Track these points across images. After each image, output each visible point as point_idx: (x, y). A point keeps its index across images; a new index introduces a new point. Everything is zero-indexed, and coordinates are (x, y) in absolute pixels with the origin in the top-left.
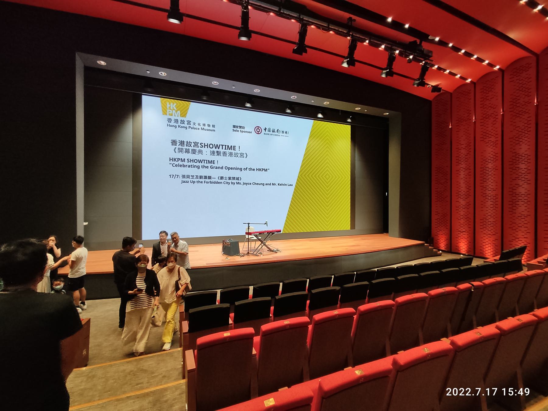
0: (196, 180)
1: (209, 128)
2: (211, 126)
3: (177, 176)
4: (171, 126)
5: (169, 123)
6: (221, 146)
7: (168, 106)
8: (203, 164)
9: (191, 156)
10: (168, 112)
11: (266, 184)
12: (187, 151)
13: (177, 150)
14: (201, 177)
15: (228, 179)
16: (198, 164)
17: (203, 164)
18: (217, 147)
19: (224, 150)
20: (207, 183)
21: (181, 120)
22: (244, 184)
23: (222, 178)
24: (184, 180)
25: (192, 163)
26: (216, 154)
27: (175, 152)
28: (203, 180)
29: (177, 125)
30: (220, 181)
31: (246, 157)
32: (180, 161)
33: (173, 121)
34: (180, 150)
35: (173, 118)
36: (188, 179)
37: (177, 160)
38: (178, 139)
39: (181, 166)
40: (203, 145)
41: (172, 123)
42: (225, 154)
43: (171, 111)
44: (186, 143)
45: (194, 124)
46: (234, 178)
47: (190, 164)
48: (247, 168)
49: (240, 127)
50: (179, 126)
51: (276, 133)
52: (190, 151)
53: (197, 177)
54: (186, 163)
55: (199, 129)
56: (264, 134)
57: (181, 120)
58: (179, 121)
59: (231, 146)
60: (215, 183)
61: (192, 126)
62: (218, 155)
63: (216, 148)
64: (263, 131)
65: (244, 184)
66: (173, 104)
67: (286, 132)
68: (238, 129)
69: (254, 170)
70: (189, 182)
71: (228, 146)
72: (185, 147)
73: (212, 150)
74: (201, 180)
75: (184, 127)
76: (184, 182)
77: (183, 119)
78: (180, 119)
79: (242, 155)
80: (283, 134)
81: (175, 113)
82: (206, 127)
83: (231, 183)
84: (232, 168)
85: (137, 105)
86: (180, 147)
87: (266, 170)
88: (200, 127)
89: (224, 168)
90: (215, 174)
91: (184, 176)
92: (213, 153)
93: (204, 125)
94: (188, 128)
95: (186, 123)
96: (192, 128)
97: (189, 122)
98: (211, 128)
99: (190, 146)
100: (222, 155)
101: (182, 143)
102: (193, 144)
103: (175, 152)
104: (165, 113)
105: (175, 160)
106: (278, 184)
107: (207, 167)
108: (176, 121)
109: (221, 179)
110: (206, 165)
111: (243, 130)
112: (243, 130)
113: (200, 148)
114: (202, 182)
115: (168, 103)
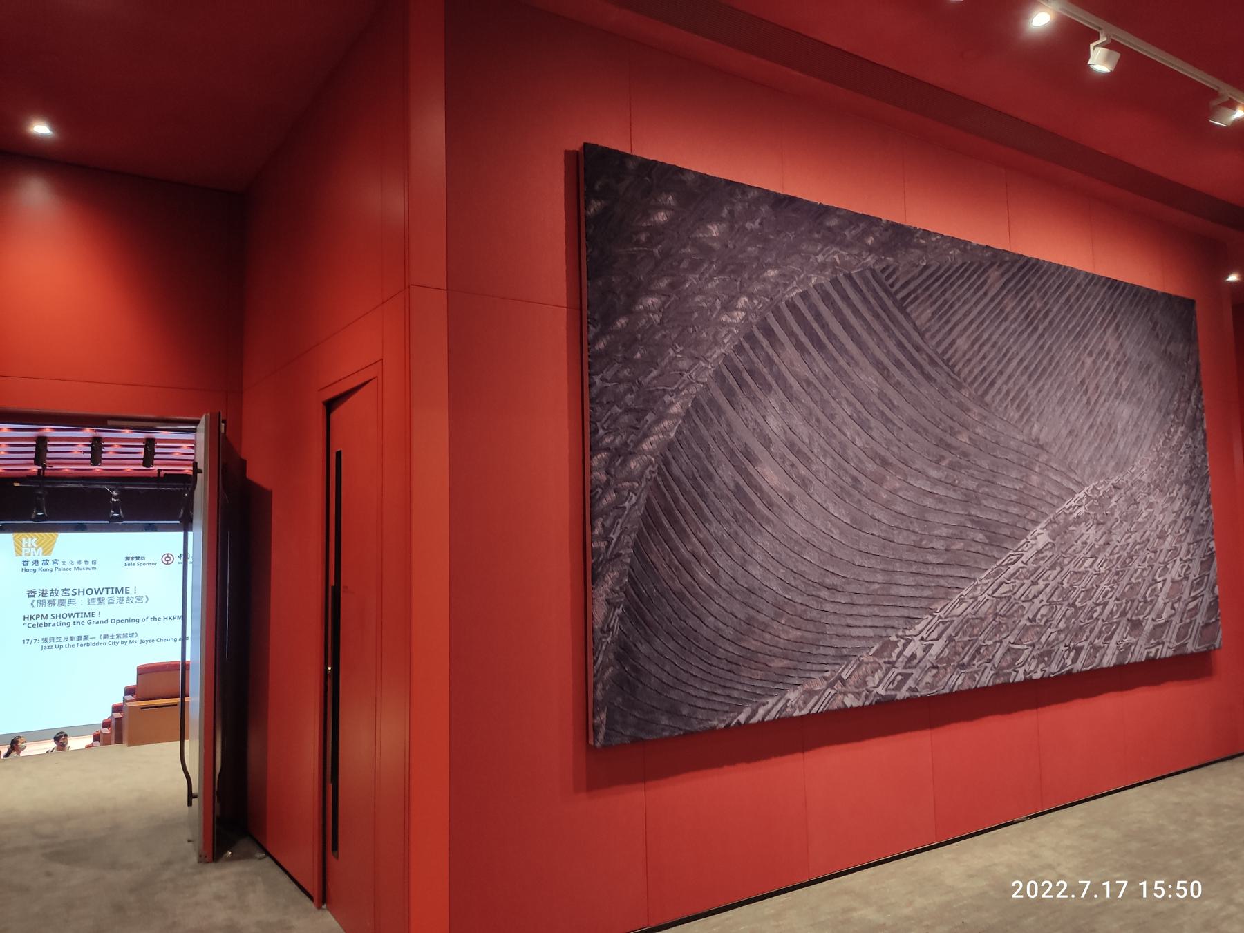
1: (86, 566)
2: (91, 562)
6: (105, 590)
20: (82, 645)
30: (103, 641)
42: (111, 600)
49: (138, 558)
63: (97, 594)
68: (133, 562)
82: (83, 565)
89: (109, 621)
98: (90, 565)
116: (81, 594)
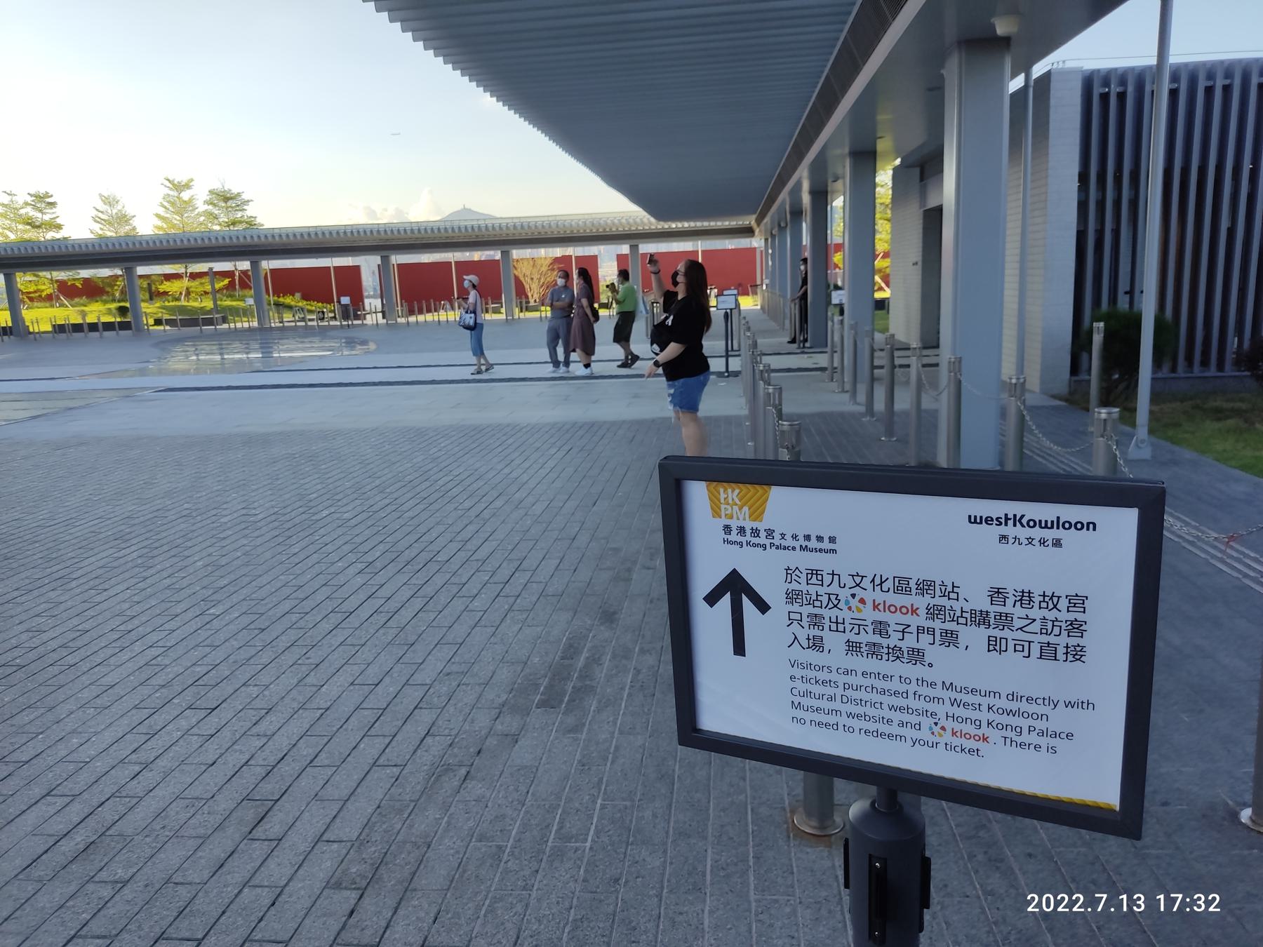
2: (826, 540)
4: (729, 542)
5: (726, 537)
7: (723, 496)
10: (723, 510)
29: (743, 540)
33: (734, 532)
35: (734, 524)
41: (734, 536)
50: (748, 543)
55: (794, 549)
57: (752, 529)
58: (748, 532)
77: (755, 525)
78: (748, 525)
81: (739, 513)
82: (813, 544)
88: (797, 545)
93: (808, 538)
94: (768, 546)
95: (763, 534)
96: (777, 548)
97: (770, 533)
98: (826, 545)
108: (742, 530)
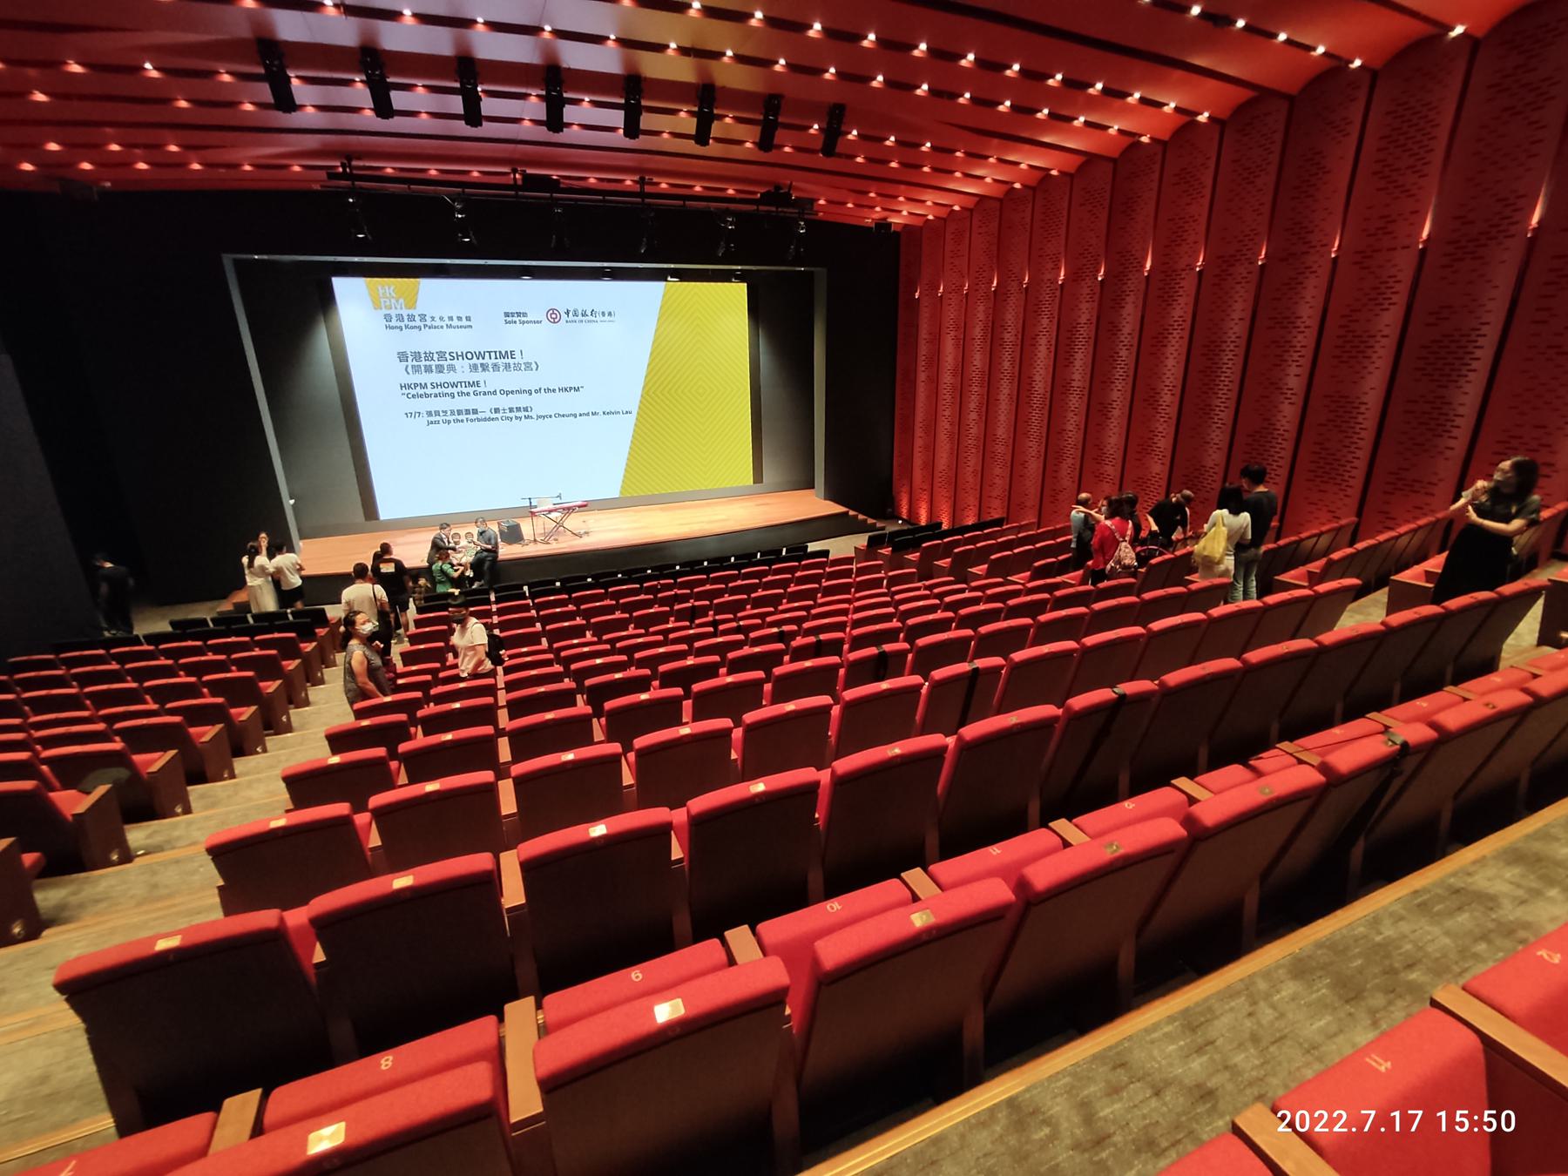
0: (451, 418)
1: (460, 323)
2: (464, 319)
3: (417, 415)
5: (387, 324)
6: (487, 354)
7: (381, 291)
8: (459, 389)
9: (435, 377)
11: (580, 415)
12: (428, 369)
13: (410, 369)
14: (460, 412)
15: (508, 411)
16: (450, 390)
17: (459, 389)
18: (480, 355)
19: (493, 361)
20: (472, 420)
21: (408, 315)
22: (539, 417)
23: (497, 410)
24: (431, 419)
25: (439, 390)
26: (480, 369)
27: (408, 373)
28: (463, 417)
29: (402, 324)
30: (494, 416)
31: (537, 369)
32: (418, 388)
33: (394, 319)
34: (416, 369)
35: (393, 313)
36: (438, 418)
37: (413, 386)
38: (409, 349)
39: (421, 396)
40: (455, 355)
43: (388, 300)
44: (423, 356)
45: (433, 318)
46: (518, 409)
47: (436, 391)
48: (540, 389)
49: (519, 314)
50: (406, 327)
51: (590, 318)
52: (434, 368)
53: (452, 413)
54: (429, 391)
55: (442, 327)
56: (567, 322)
58: (406, 318)
59: (506, 352)
60: (485, 420)
61: (428, 323)
62: (484, 370)
63: (478, 359)
64: (564, 316)
65: (539, 417)
66: (389, 288)
67: (610, 314)
68: (514, 319)
69: (554, 391)
70: (441, 422)
71: (500, 352)
72: (424, 363)
73: (472, 362)
74: (460, 417)
75: (415, 327)
76: (432, 423)
77: (410, 312)
78: (405, 313)
79: (528, 366)
80: (603, 319)
82: (455, 322)
83: (514, 418)
84: (512, 392)
85: (327, 300)
86: (415, 363)
87: (577, 390)
88: (444, 324)
89: (498, 392)
90: (484, 404)
91: (429, 414)
92: (474, 368)
93: (451, 318)
95: (417, 318)
97: (423, 317)
98: (464, 322)
99: (432, 359)
100: (491, 370)
101: (417, 356)
102: (436, 356)
103: (408, 373)
104: (377, 306)
105: (410, 387)
106: (604, 413)
107: (468, 394)
108: (400, 318)
109: (496, 412)
110: (465, 390)
111: (525, 319)
112: (525, 319)
113: (449, 362)
114: (462, 421)
115: (380, 288)
116: (460, 358)
